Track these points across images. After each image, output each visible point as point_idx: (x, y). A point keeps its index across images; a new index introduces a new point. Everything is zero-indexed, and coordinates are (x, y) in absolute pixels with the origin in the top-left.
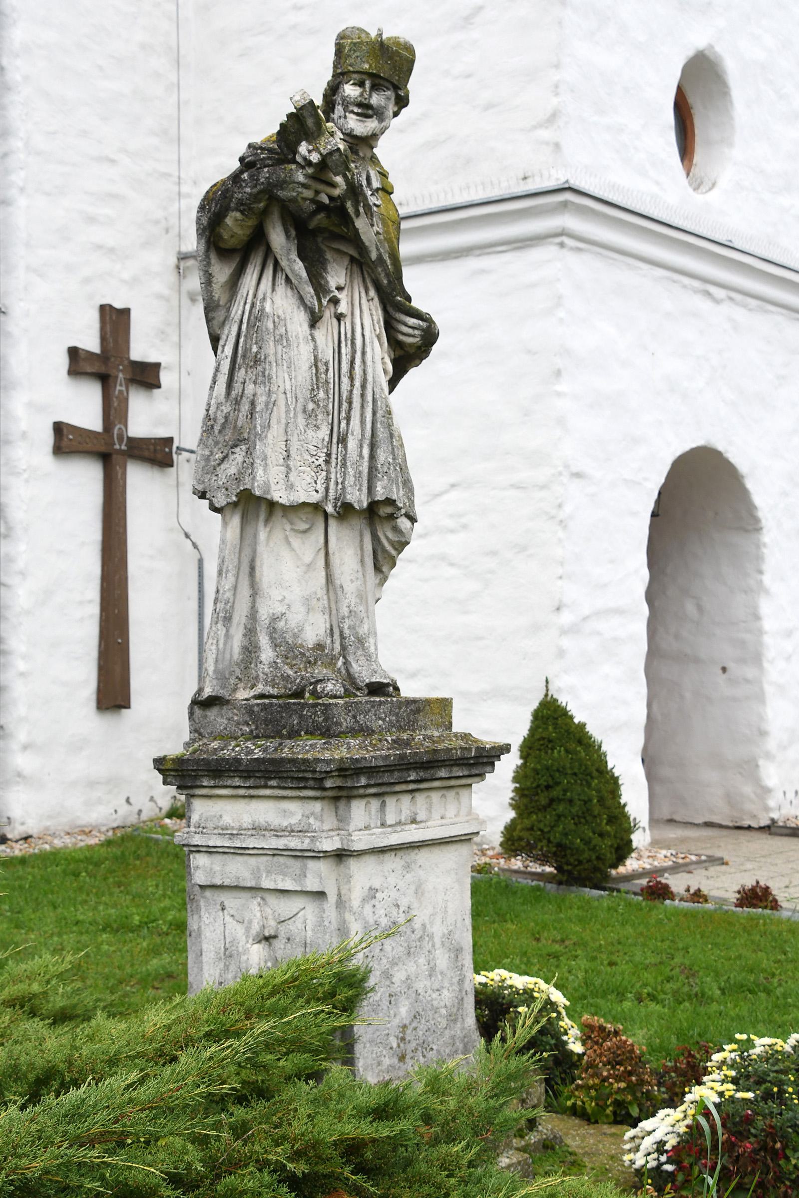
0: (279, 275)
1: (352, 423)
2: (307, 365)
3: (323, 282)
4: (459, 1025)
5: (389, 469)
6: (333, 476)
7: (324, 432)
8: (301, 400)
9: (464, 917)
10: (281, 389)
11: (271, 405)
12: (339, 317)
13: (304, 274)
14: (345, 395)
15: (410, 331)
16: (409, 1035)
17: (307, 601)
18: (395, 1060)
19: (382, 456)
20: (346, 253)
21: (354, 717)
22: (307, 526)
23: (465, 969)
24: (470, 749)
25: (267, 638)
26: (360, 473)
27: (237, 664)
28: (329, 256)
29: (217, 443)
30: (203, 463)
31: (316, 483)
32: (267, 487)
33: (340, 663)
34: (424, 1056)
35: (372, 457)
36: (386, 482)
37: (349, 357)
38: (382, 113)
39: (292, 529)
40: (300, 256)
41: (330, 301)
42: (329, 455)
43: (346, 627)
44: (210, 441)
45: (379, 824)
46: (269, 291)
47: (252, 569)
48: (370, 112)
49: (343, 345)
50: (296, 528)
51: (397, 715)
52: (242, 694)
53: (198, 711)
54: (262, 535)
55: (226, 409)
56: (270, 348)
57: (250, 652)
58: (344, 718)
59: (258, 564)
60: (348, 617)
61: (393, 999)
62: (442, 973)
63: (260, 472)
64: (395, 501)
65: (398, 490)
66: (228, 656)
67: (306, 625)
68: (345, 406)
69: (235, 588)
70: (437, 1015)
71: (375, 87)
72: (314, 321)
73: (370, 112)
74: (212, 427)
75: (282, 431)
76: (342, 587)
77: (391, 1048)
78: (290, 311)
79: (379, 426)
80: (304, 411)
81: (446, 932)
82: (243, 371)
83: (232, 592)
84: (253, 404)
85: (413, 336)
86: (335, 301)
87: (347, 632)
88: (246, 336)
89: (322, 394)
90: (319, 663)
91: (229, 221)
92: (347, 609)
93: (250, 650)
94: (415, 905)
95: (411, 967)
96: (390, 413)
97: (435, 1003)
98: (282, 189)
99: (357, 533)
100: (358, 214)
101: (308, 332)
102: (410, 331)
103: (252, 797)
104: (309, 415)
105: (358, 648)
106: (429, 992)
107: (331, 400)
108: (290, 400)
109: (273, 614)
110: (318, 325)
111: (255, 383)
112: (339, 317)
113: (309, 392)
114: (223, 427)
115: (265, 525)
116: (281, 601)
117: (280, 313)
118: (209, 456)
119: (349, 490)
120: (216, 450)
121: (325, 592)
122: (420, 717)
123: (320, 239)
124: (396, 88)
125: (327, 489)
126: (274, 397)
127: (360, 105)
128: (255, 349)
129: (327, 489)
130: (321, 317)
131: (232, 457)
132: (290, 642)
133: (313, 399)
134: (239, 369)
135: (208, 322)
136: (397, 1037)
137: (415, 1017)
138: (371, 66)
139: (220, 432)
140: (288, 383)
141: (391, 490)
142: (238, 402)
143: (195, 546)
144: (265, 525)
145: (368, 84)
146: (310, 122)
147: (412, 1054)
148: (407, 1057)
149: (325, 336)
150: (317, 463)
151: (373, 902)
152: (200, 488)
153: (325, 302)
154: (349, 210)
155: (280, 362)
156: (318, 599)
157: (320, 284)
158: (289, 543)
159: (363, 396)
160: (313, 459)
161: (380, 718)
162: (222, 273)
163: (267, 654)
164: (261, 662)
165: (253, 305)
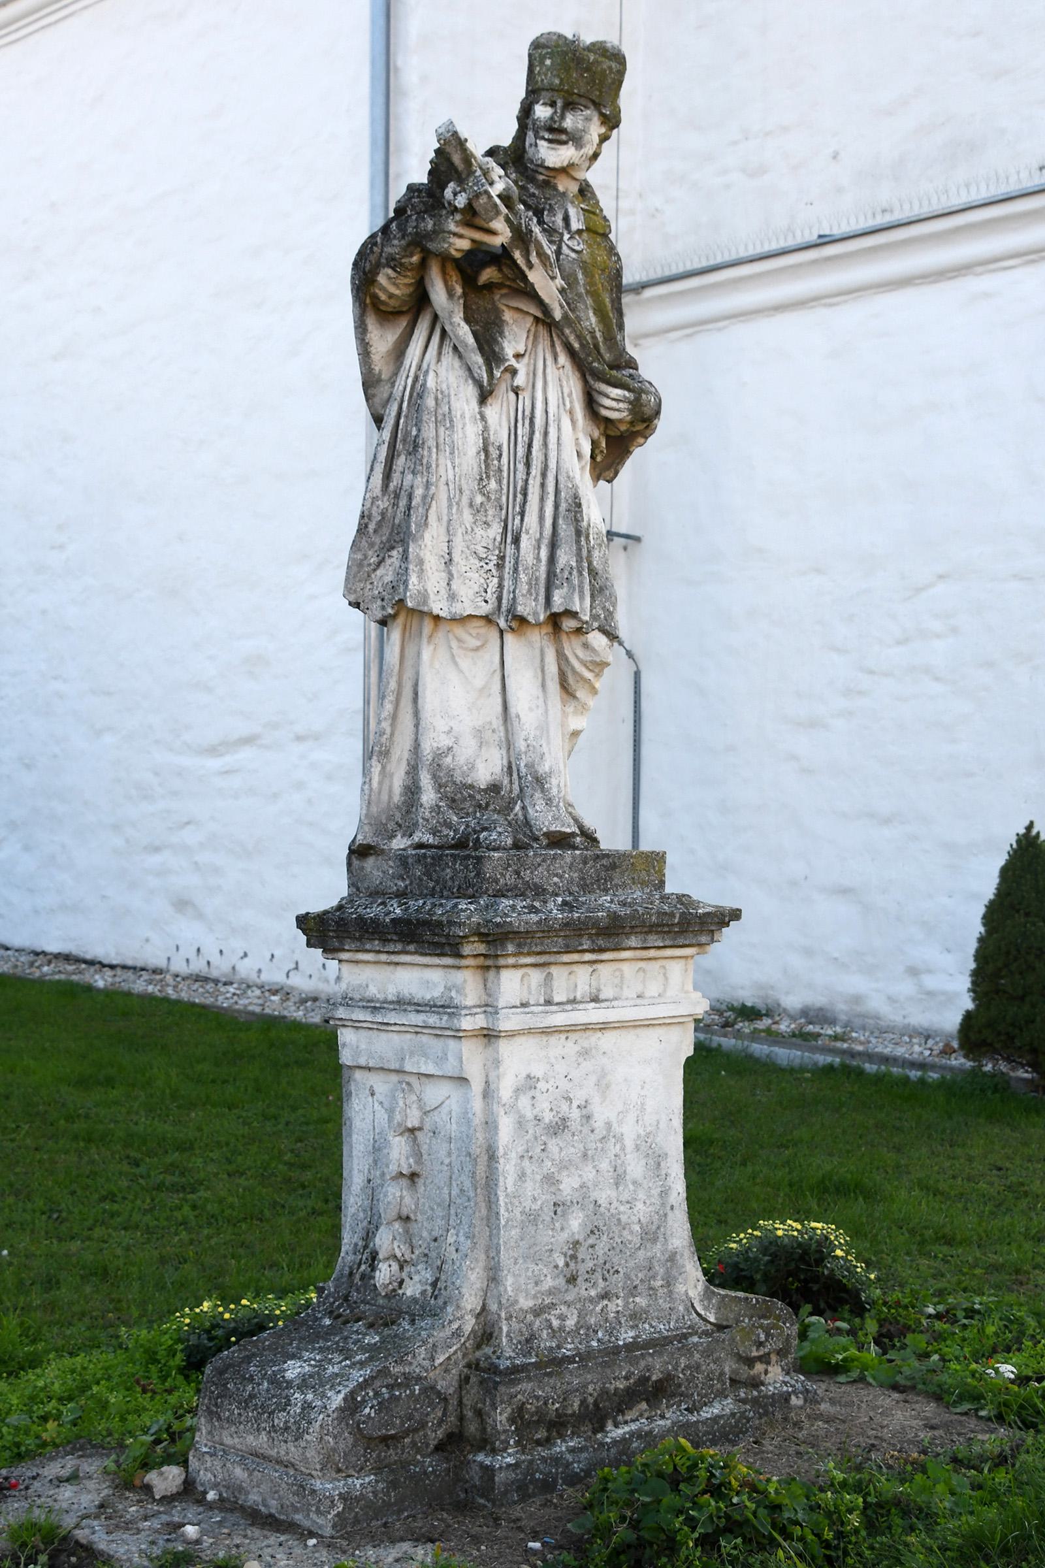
0: (447, 342)
1: (526, 519)
3: (497, 350)
4: (659, 1245)
5: (570, 573)
6: (506, 583)
7: (496, 530)
8: (467, 493)
9: (671, 1116)
10: (443, 479)
11: (427, 500)
12: (516, 391)
13: (471, 340)
14: (520, 484)
15: (614, 404)
17: (478, 733)
18: (561, 1281)
19: (565, 557)
20: (528, 313)
21: (517, 873)
22: (478, 643)
23: (670, 1179)
26: (537, 579)
27: (398, 807)
28: (508, 316)
29: (372, 545)
30: (355, 569)
32: (424, 596)
33: (517, 808)
34: (605, 1279)
35: (552, 559)
36: (565, 590)
37: (526, 439)
38: (581, 138)
40: (467, 320)
41: (506, 370)
42: (502, 558)
43: (522, 765)
44: (364, 543)
45: (542, 1001)
46: (434, 361)
47: (416, 694)
48: (564, 137)
49: (520, 425)
51: (581, 870)
52: (399, 843)
53: (356, 862)
54: (426, 654)
55: (384, 504)
56: (428, 432)
57: (412, 793)
58: (502, 874)
59: (420, 689)
60: (526, 753)
61: (559, 1210)
62: (635, 1183)
63: (413, 579)
65: (582, 598)
66: (385, 797)
68: (519, 497)
69: (394, 717)
70: (625, 1233)
71: (570, 106)
72: (484, 396)
73: (564, 137)
74: (366, 526)
75: (443, 530)
76: (518, 716)
77: (556, 1267)
78: (455, 385)
79: (561, 521)
80: (471, 505)
81: (643, 1133)
82: (402, 458)
83: (390, 722)
84: (410, 497)
86: (514, 372)
87: (523, 770)
88: (406, 417)
89: (493, 485)
90: (492, 807)
91: (382, 279)
93: (412, 791)
95: (589, 1174)
96: (579, 505)
97: (624, 1218)
98: (431, 240)
99: (537, 652)
100: (530, 266)
101: (477, 410)
102: (614, 404)
104: (477, 510)
107: (505, 491)
108: (452, 492)
109: (438, 749)
110: (490, 400)
111: (413, 473)
112: (516, 391)
113: (476, 482)
114: (379, 525)
115: (429, 642)
117: (444, 387)
118: (362, 560)
119: (520, 600)
120: (370, 553)
121: (501, 722)
122: (616, 875)
123: (497, 297)
124: (597, 105)
125: (499, 599)
126: (433, 489)
127: (551, 130)
128: (414, 433)
129: (499, 599)
130: (491, 393)
131: (388, 561)
133: (482, 490)
134: (399, 456)
135: (367, 400)
136: (565, 1255)
137: (592, 1232)
138: (561, 80)
139: (375, 531)
140: (451, 472)
142: (397, 496)
143: (629, 654)
144: (429, 642)
145: (559, 104)
146: (456, 159)
147: (587, 1276)
148: (580, 1279)
149: (498, 413)
150: (487, 567)
151: (532, 1093)
152: (352, 598)
153: (497, 374)
155: (442, 447)
156: (494, 731)
157: (494, 351)
158: (456, 664)
159: (543, 485)
160: (482, 564)
161: (556, 875)
162: (382, 340)
163: (429, 796)
164: (421, 805)
165: (416, 378)
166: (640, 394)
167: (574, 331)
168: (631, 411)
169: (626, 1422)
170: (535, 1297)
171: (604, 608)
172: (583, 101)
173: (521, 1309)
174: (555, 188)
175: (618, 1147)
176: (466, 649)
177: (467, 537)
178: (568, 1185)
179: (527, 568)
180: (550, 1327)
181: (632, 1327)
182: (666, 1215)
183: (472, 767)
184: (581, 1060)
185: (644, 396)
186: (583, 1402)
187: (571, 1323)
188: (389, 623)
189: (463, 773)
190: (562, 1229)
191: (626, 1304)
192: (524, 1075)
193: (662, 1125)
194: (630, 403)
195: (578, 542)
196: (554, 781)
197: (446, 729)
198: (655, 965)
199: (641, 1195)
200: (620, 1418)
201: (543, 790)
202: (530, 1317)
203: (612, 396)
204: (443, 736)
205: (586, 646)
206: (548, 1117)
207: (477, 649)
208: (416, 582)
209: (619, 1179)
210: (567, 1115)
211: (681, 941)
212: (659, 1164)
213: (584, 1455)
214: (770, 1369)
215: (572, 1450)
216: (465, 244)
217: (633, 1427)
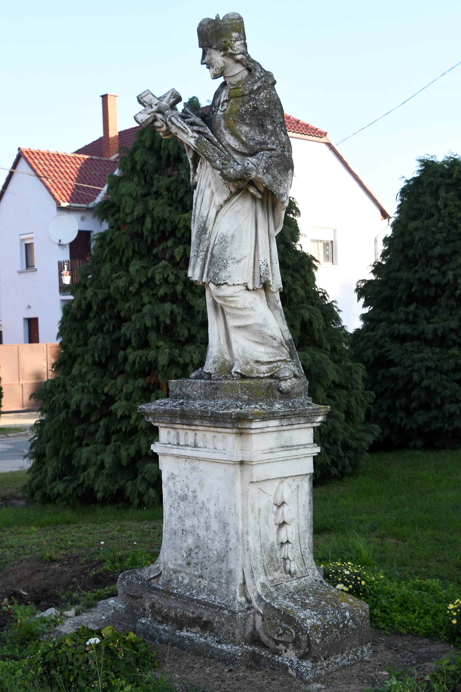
4: (224, 564)
9: (231, 507)
16: (193, 555)
18: (184, 563)
23: (230, 536)
24: (207, 412)
34: (202, 570)
38: (211, 63)
45: (175, 443)
51: (204, 389)
62: (214, 532)
70: (210, 553)
77: (183, 556)
81: (218, 511)
94: (198, 490)
97: (210, 546)
103: (301, 428)
106: (206, 539)
122: (218, 392)
148: (191, 565)
151: (174, 481)
161: (195, 391)
169: (191, 632)
170: (174, 565)
173: (169, 568)
175: (207, 513)
178: (188, 523)
180: (178, 579)
181: (208, 595)
182: (228, 551)
184: (192, 471)
185: (224, 171)
186: (176, 614)
187: (186, 582)
190: (185, 541)
191: (209, 584)
192: (170, 473)
193: (226, 510)
198: (220, 436)
199: (217, 538)
200: (189, 629)
202: (171, 572)
206: (180, 492)
209: (208, 528)
210: (187, 493)
211: (218, 425)
212: (225, 527)
213: (167, 634)
214: (288, 650)
215: (164, 630)
217: (192, 635)
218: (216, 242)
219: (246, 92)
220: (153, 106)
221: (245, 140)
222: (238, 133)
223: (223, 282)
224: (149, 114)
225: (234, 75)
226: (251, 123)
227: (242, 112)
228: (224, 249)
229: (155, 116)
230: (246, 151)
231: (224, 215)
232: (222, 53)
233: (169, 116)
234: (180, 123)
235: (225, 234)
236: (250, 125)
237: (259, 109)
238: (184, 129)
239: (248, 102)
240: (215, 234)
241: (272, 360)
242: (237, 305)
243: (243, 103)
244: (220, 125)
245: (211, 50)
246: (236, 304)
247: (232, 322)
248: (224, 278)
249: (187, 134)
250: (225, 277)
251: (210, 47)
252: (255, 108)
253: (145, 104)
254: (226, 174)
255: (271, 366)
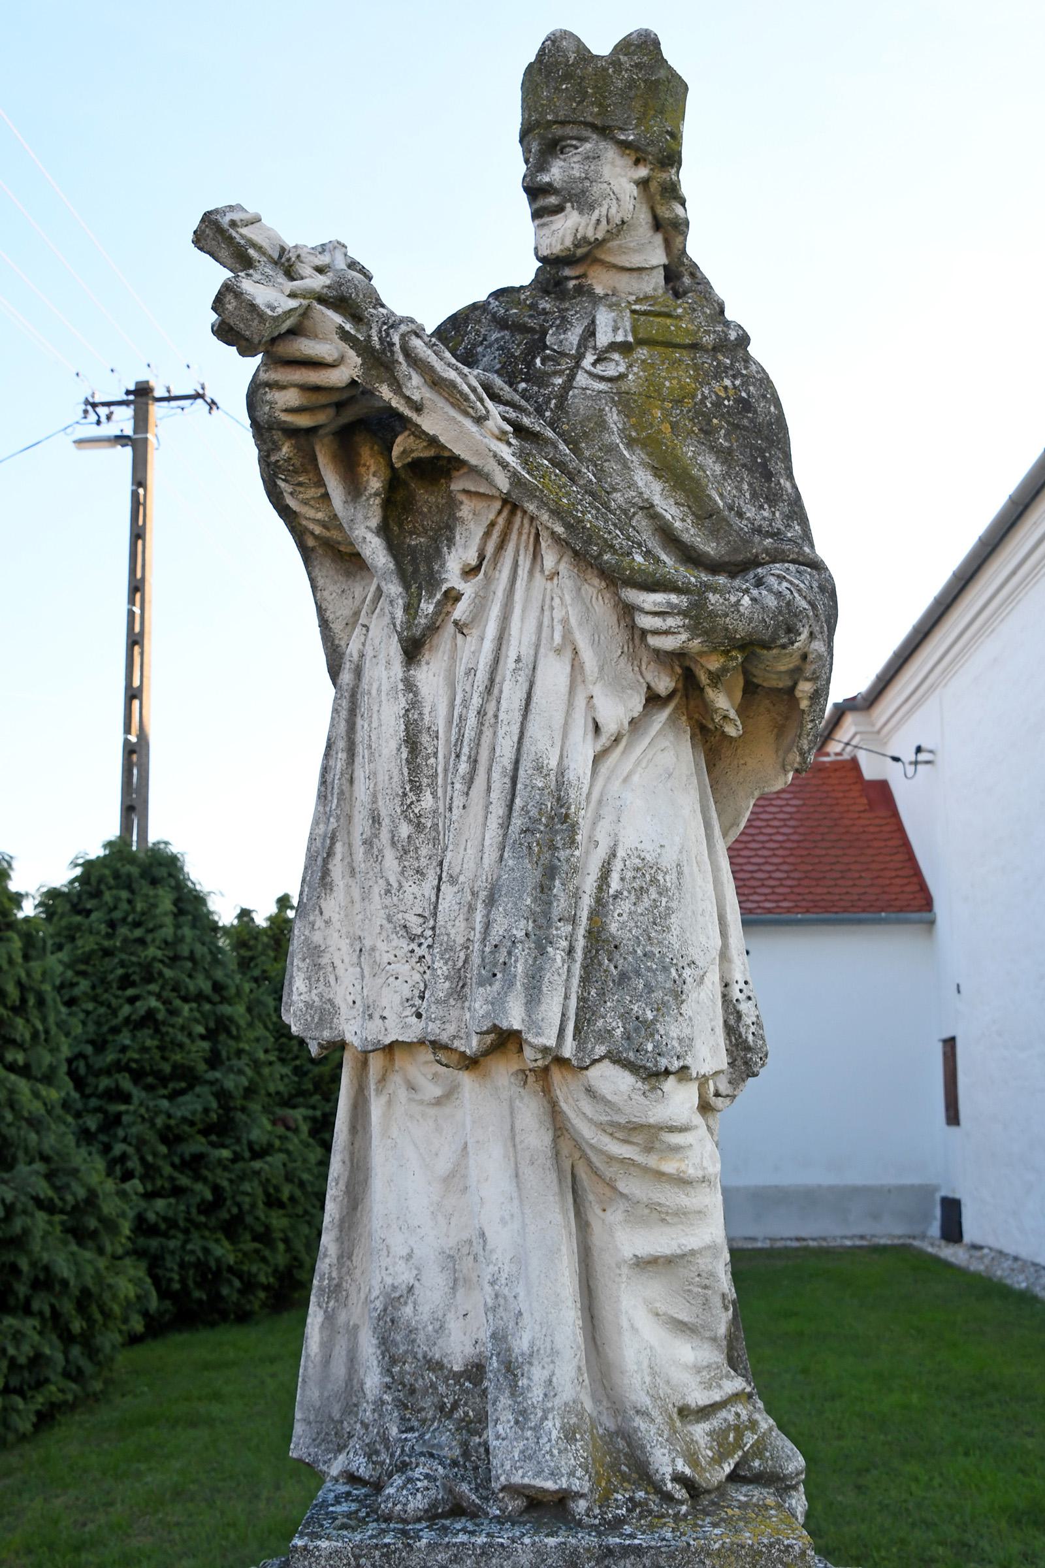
2: (393, 745)
3: (436, 567)
8: (386, 822)
25: (375, 1342)
31: (422, 998)
38: (583, 192)
39: (410, 1100)
48: (553, 200)
50: (418, 1097)
64: (519, 1032)
67: (450, 1316)
72: (413, 649)
73: (553, 200)
78: (377, 642)
80: (393, 844)
85: (667, 632)
92: (488, 1289)
101: (400, 675)
104: (405, 851)
105: (499, 1389)
109: (394, 1288)
113: (398, 801)
116: (409, 1257)
132: (420, 1356)
141: (505, 1011)
144: (379, 1092)
150: (420, 952)
154: (394, 404)
160: (414, 946)
166: (701, 594)
167: (543, 504)
168: (694, 629)
171: (625, 1016)
172: (570, 130)
174: (590, 293)
176: (421, 1102)
177: (388, 901)
179: (451, 949)
183: (441, 1329)
185: (713, 598)
188: (398, 1055)
189: (428, 1337)
194: (684, 614)
195: (544, 889)
196: (538, 1374)
197: (404, 1252)
201: (514, 1390)
203: (647, 607)
204: (401, 1262)
205: (590, 1091)
207: (438, 1102)
208: (303, 989)
216: (291, 397)
218: (615, 884)
219: (708, 340)
220: (306, 270)
221: (721, 504)
222: (694, 472)
223: (676, 1065)
224: (293, 295)
225: (640, 270)
226: (730, 451)
227: (703, 401)
228: (659, 919)
229: (306, 312)
230: (710, 548)
231: (626, 780)
232: (643, 172)
233: (403, 328)
234: (457, 369)
235: (648, 858)
236: (725, 456)
237: (755, 412)
238: (472, 397)
239: (718, 377)
240: (601, 854)
241: (717, 1396)
242: (683, 1167)
243: (703, 377)
244: (602, 425)
245: (602, 145)
246: (682, 1160)
247: (626, 1240)
248: (675, 1043)
249: (480, 420)
250: (680, 1040)
251: (604, 131)
252: (745, 405)
253: (251, 252)
254: (720, 609)
255: (715, 1422)
